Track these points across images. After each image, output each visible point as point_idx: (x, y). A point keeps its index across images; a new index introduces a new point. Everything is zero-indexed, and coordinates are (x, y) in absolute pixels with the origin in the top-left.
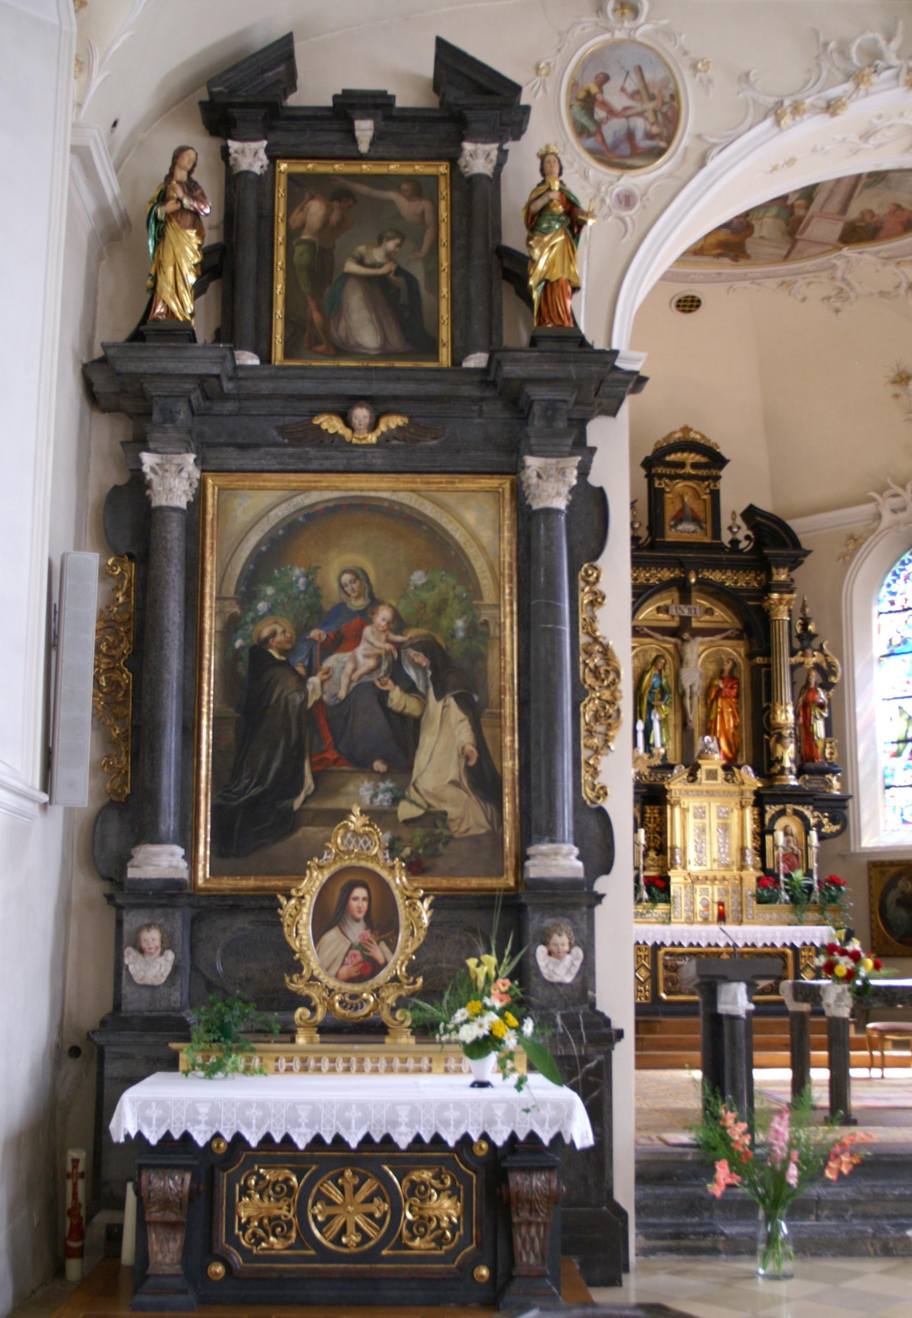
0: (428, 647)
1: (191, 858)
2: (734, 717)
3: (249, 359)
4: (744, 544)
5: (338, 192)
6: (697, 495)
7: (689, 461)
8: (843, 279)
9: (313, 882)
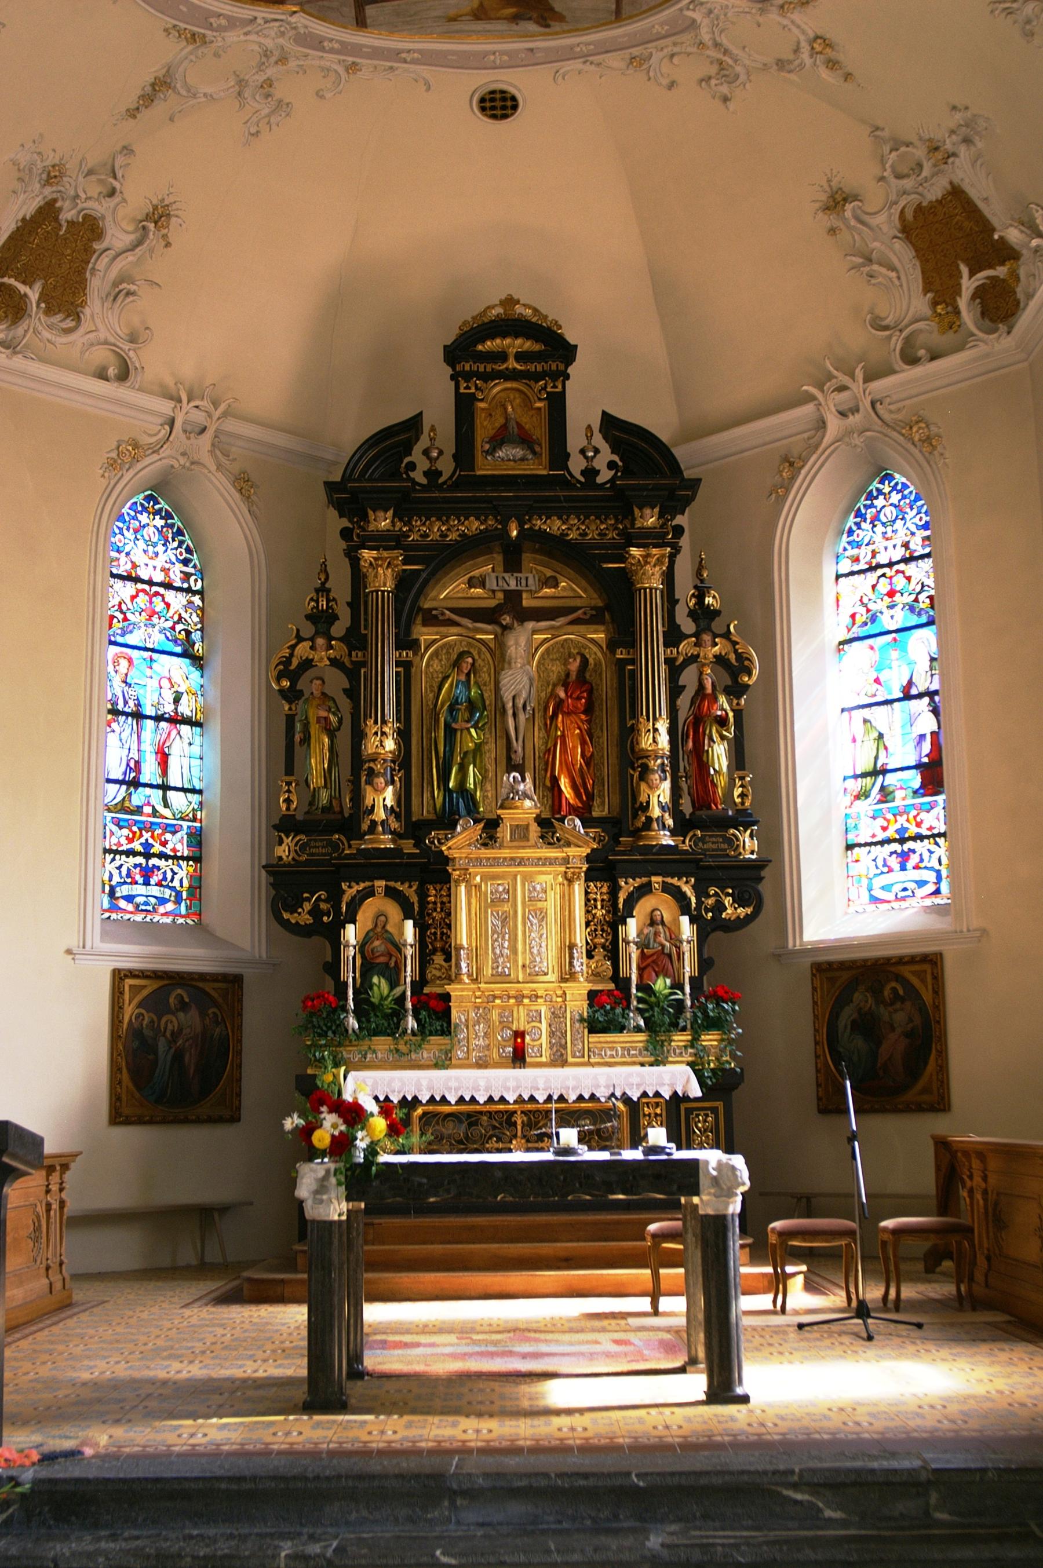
2: (583, 743)
4: (605, 476)
6: (527, 402)
7: (512, 351)
8: (717, 45)
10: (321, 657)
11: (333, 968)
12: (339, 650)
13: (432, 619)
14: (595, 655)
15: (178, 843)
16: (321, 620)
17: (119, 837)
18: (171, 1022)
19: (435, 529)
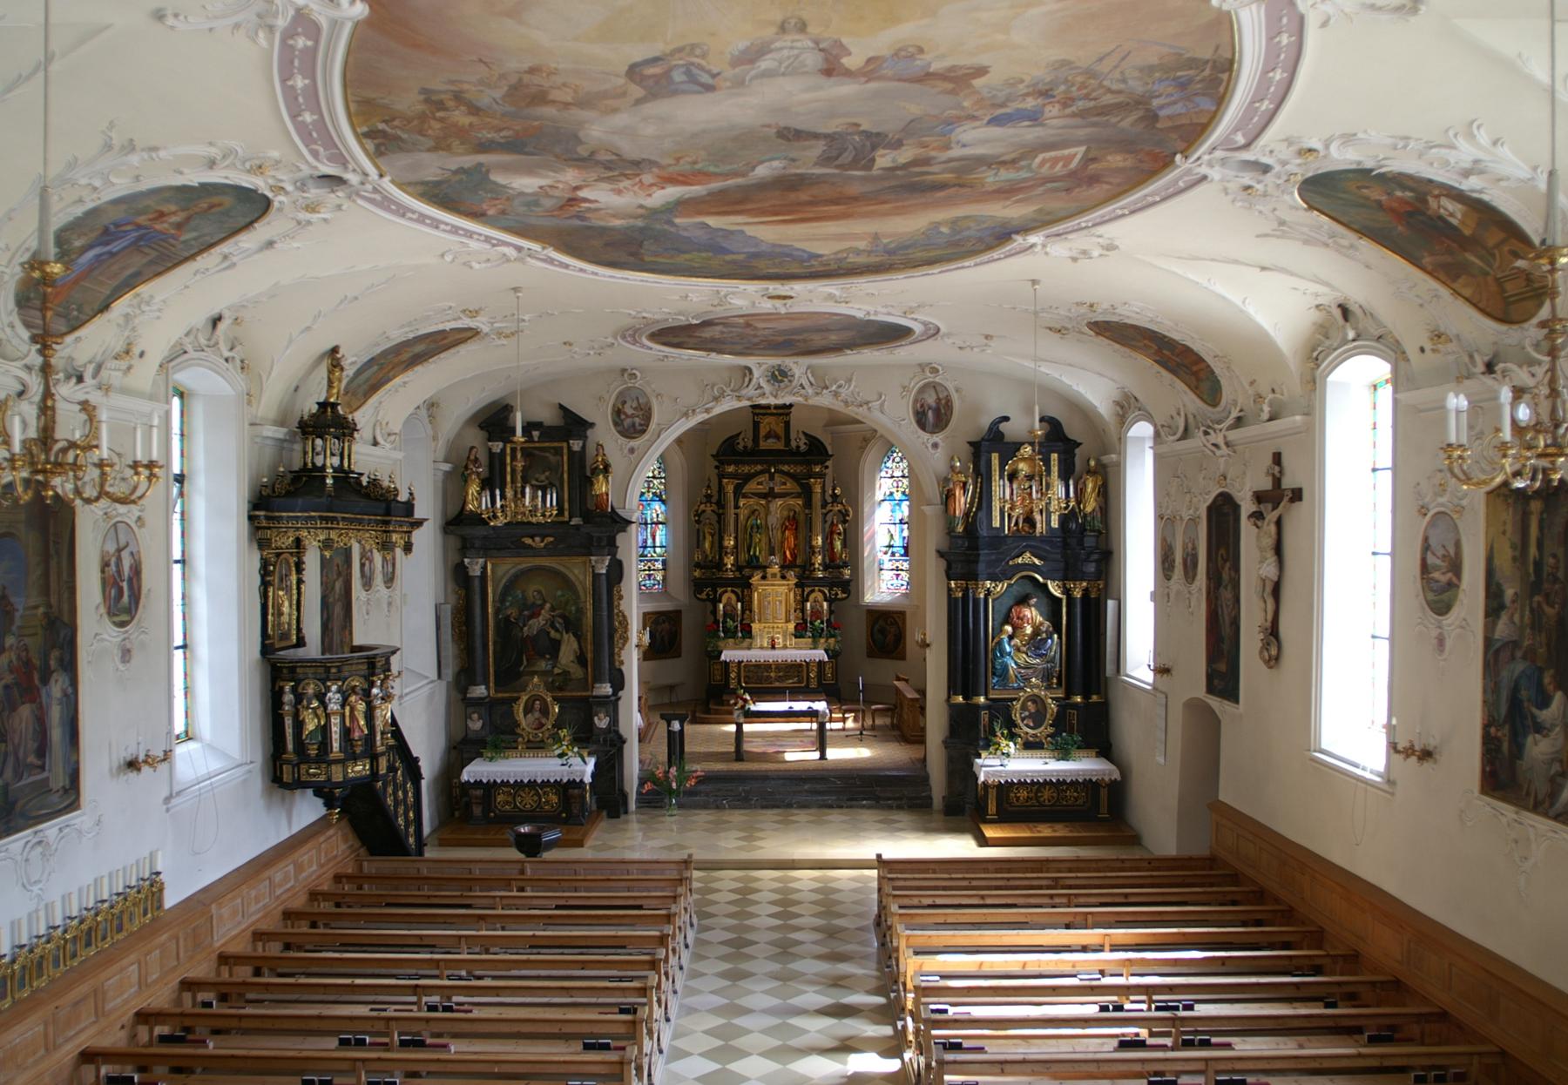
0: (563, 616)
1: (488, 688)
9: (525, 698)
10: (709, 509)
12: (714, 507)
13: (745, 496)
15: (659, 565)
16: (708, 497)
17: (641, 566)
19: (746, 469)
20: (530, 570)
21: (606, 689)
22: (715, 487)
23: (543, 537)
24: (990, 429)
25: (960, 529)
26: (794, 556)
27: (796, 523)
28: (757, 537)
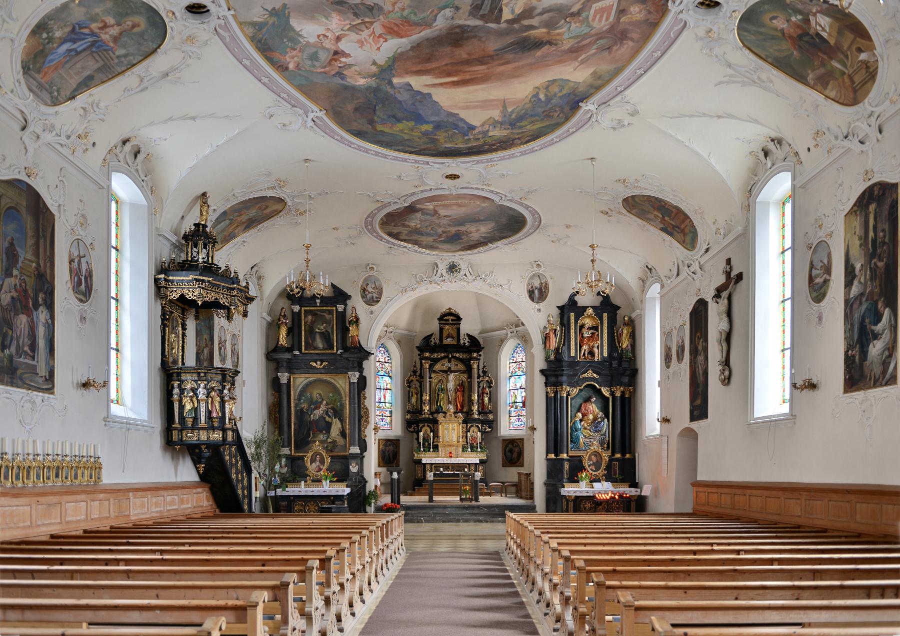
0: (333, 409)
3: (297, 353)
4: (467, 344)
5: (314, 313)
9: (310, 455)
11: (418, 439)
13: (435, 372)
14: (464, 379)
15: (388, 414)
16: (415, 372)
17: (378, 413)
18: (387, 449)
20: (315, 381)
21: (355, 450)
22: (418, 366)
23: (322, 362)
24: (570, 299)
25: (552, 357)
26: (462, 407)
27: (464, 388)
28: (442, 395)
